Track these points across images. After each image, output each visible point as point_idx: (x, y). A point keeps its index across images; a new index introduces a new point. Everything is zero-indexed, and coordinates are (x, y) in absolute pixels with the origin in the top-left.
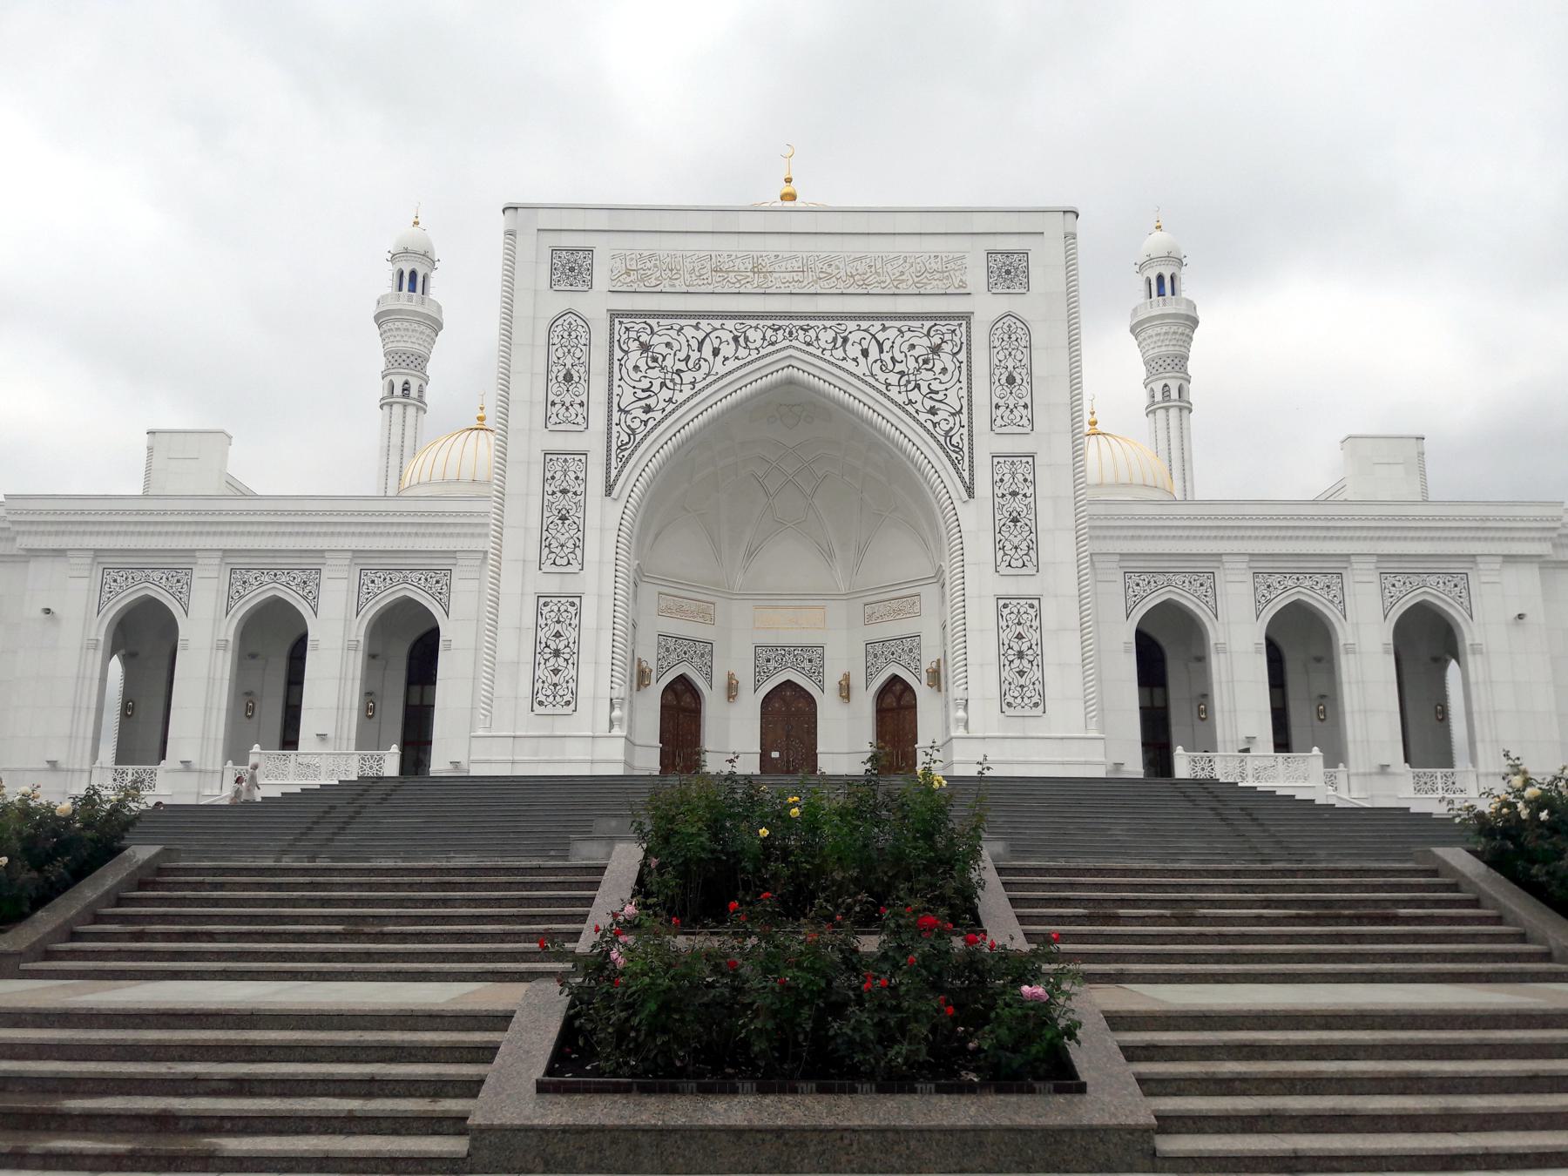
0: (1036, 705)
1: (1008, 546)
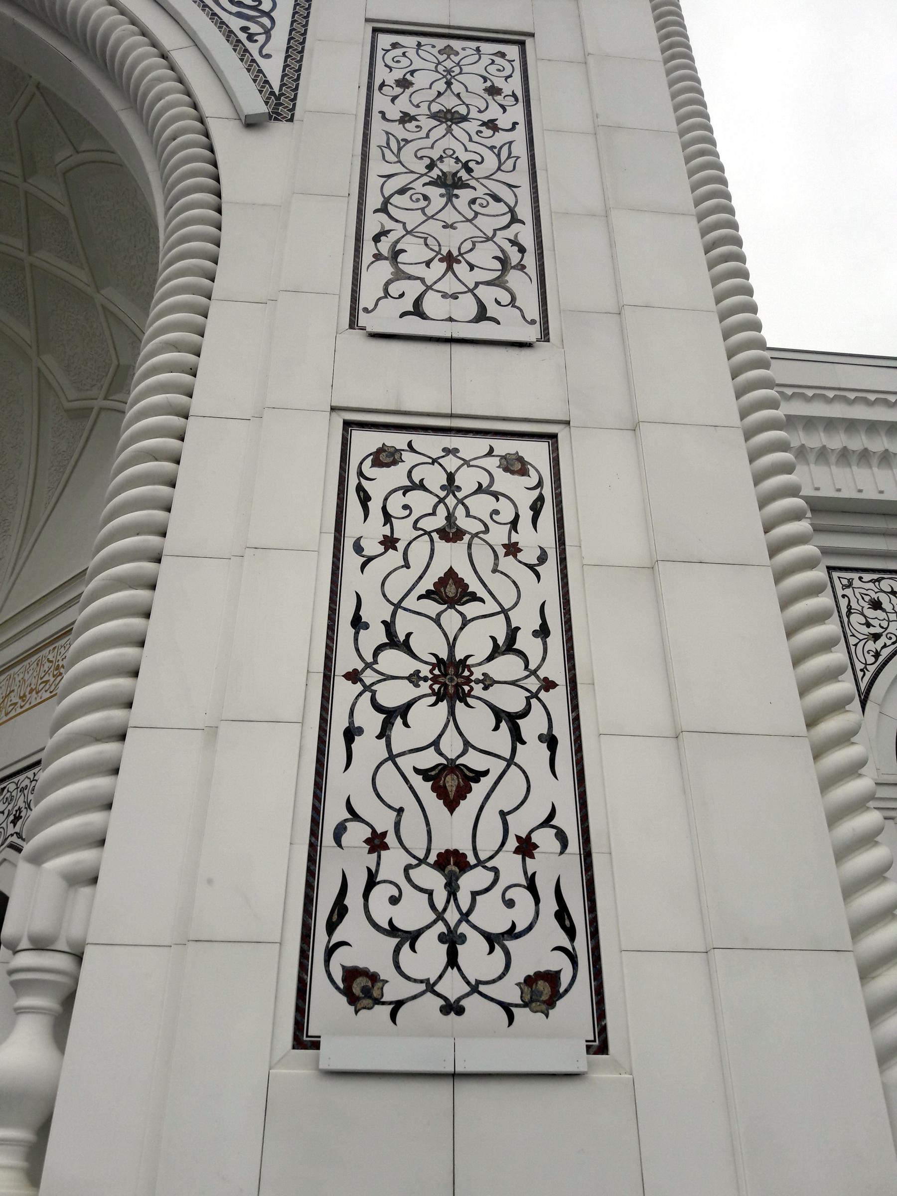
0: (543, 991)
1: (414, 252)
